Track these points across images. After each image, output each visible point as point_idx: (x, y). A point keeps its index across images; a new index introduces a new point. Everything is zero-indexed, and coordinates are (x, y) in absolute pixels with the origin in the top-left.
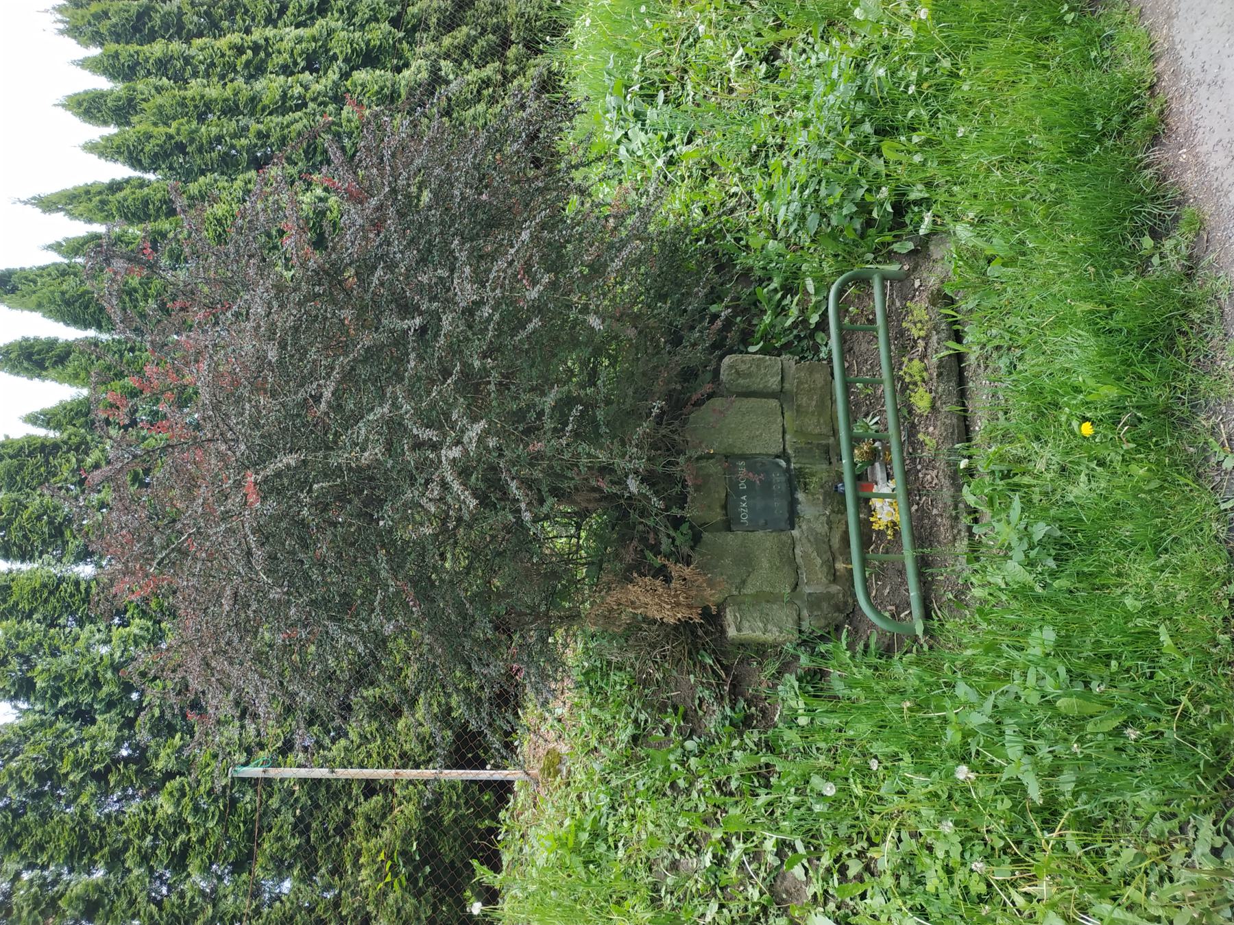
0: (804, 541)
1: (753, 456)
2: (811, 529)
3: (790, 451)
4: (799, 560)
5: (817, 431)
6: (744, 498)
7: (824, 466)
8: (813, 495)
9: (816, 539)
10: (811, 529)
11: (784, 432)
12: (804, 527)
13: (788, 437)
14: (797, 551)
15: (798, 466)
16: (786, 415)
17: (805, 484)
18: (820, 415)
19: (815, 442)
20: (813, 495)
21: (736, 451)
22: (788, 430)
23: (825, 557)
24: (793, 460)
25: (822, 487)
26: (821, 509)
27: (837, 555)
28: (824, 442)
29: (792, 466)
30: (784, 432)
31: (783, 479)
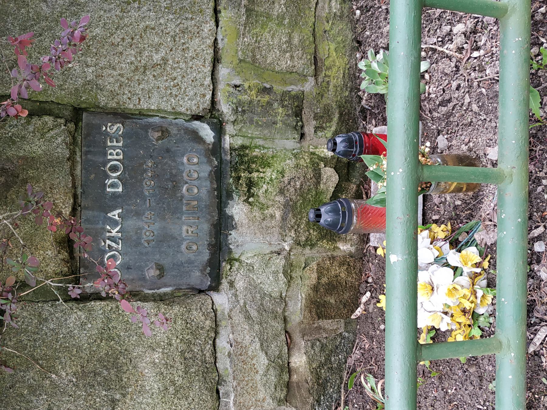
0: (238, 318)
1: (142, 114)
2: (253, 287)
3: (225, 108)
4: (224, 364)
5: (285, 63)
6: (115, 214)
7: (291, 143)
8: (263, 207)
9: (261, 309)
10: (253, 287)
11: (216, 60)
12: (240, 284)
13: (223, 71)
14: (222, 343)
15: (239, 142)
16: (224, 16)
17: (251, 184)
18: (294, 24)
19: (278, 88)
20: (263, 207)
21: (103, 100)
22: (226, 57)
23: (274, 349)
24: (229, 129)
25: (282, 192)
26: (275, 239)
27: (297, 337)
28: (294, 89)
29: (227, 141)
30: (216, 60)
31: (206, 170)
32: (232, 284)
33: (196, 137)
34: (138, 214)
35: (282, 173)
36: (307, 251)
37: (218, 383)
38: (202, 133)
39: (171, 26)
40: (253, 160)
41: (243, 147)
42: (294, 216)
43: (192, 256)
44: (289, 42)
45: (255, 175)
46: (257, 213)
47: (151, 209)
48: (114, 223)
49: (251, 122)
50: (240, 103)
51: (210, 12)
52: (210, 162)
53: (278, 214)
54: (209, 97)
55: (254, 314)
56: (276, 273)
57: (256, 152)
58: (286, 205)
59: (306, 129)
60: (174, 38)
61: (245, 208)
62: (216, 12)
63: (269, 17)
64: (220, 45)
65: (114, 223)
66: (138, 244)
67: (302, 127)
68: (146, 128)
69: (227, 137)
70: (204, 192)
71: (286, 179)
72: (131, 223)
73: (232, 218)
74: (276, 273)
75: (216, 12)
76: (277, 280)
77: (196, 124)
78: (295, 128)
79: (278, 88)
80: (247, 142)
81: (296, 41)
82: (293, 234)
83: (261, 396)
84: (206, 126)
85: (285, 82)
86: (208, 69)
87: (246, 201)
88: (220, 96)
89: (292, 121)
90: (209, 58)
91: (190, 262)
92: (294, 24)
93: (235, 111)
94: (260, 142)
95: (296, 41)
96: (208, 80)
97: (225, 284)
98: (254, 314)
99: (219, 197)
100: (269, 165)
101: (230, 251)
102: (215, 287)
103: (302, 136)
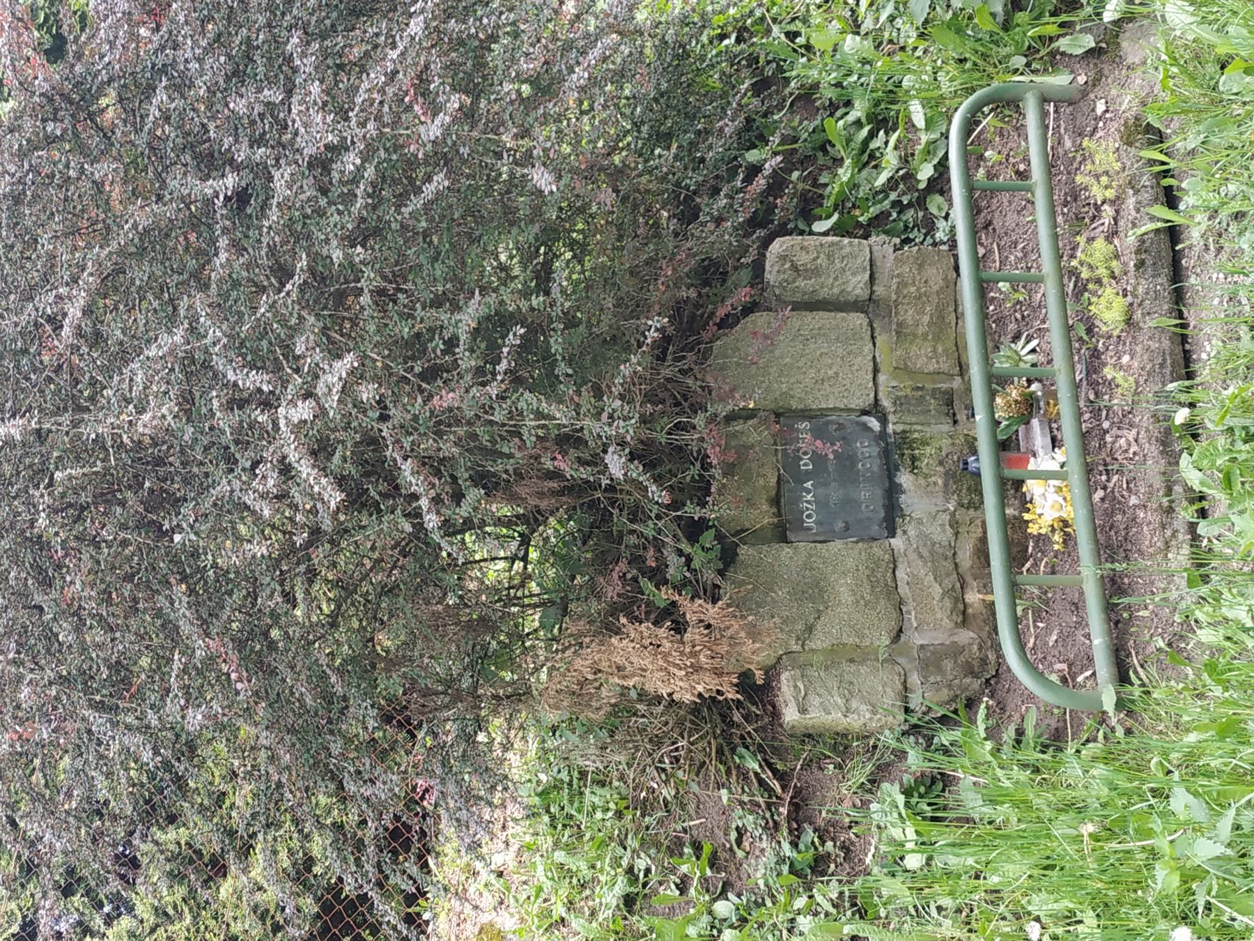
0: (913, 556)
1: (823, 412)
2: (922, 536)
3: (886, 403)
4: (904, 590)
5: (933, 366)
6: (808, 485)
7: (946, 428)
8: (926, 476)
9: (932, 553)
10: (922, 536)
11: (876, 371)
12: (912, 533)
13: (882, 378)
14: (900, 574)
15: (900, 428)
16: (879, 340)
17: (914, 459)
18: (937, 339)
19: (929, 386)
20: (926, 476)
21: (794, 405)
22: (882, 368)
23: (948, 583)
24: (891, 418)
25: (941, 463)
26: (940, 501)
27: (969, 579)
28: (944, 386)
29: (890, 428)
30: (876, 371)
31: (875, 450)
32: (905, 532)
33: (866, 428)
34: (826, 485)
35: (940, 449)
36: (971, 511)
37: (900, 603)
38: (870, 425)
39: (840, 351)
40: (914, 440)
41: (904, 432)
42: (955, 483)
43: (870, 514)
44: (935, 351)
45: (917, 452)
46: (922, 481)
47: (835, 480)
48: (808, 491)
49: (909, 411)
50: (898, 398)
51: (868, 337)
52: (878, 445)
53: (940, 482)
54: (872, 395)
55: (926, 554)
56: (942, 525)
57: (916, 435)
58: (946, 474)
59: (958, 417)
60: (842, 358)
61: (911, 477)
62: (873, 337)
63: (915, 335)
64: (878, 360)
65: (808, 491)
66: (827, 505)
67: (954, 415)
68: (827, 423)
69: (890, 425)
70: (876, 469)
71: (944, 454)
72: (821, 491)
73: (901, 485)
74: (942, 525)
75: (873, 337)
76: (944, 531)
77: (865, 418)
78: (947, 414)
79: (929, 386)
80: (907, 428)
81: (940, 350)
82: (955, 497)
83: (939, 616)
84: (873, 419)
85: (935, 382)
86: (870, 376)
87: (912, 472)
88: (881, 395)
89: (945, 409)
90: (870, 368)
91: (869, 519)
92: (937, 339)
93: (895, 404)
94: (919, 428)
95: (940, 350)
96: (871, 384)
97: (899, 532)
98: (926, 554)
99: (888, 470)
100: (928, 444)
101: (902, 510)
102: (892, 534)
103: (955, 422)
